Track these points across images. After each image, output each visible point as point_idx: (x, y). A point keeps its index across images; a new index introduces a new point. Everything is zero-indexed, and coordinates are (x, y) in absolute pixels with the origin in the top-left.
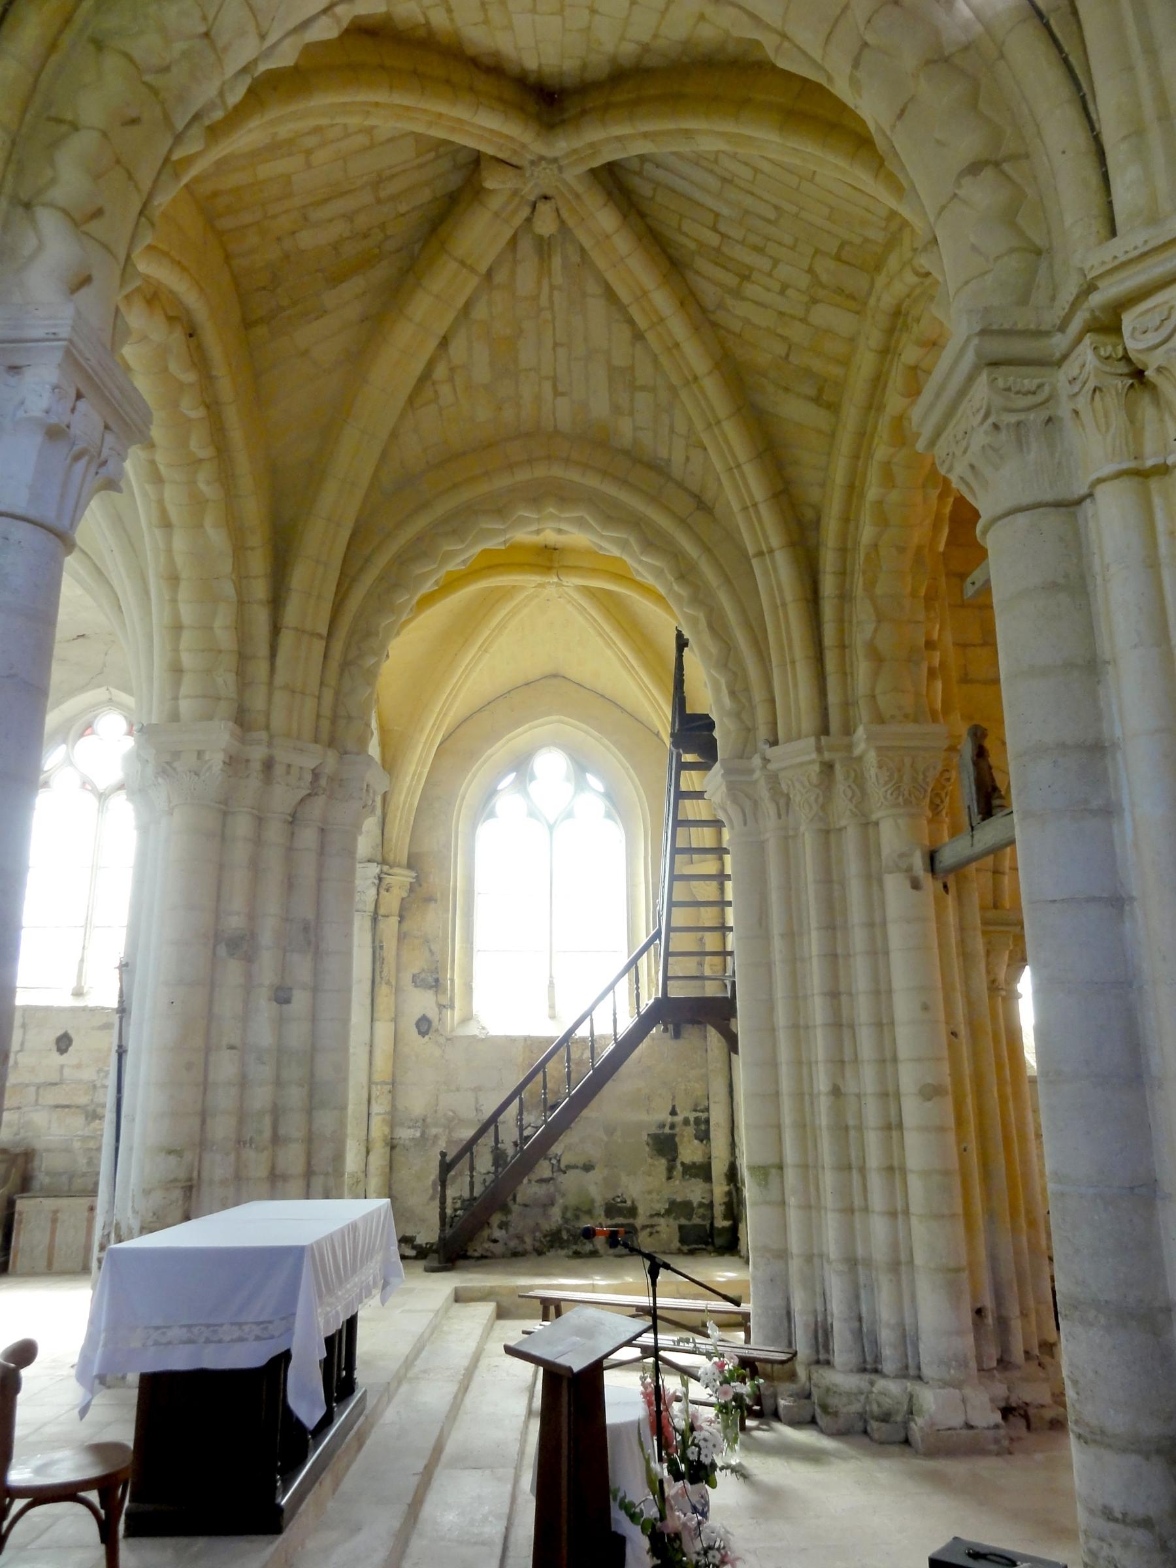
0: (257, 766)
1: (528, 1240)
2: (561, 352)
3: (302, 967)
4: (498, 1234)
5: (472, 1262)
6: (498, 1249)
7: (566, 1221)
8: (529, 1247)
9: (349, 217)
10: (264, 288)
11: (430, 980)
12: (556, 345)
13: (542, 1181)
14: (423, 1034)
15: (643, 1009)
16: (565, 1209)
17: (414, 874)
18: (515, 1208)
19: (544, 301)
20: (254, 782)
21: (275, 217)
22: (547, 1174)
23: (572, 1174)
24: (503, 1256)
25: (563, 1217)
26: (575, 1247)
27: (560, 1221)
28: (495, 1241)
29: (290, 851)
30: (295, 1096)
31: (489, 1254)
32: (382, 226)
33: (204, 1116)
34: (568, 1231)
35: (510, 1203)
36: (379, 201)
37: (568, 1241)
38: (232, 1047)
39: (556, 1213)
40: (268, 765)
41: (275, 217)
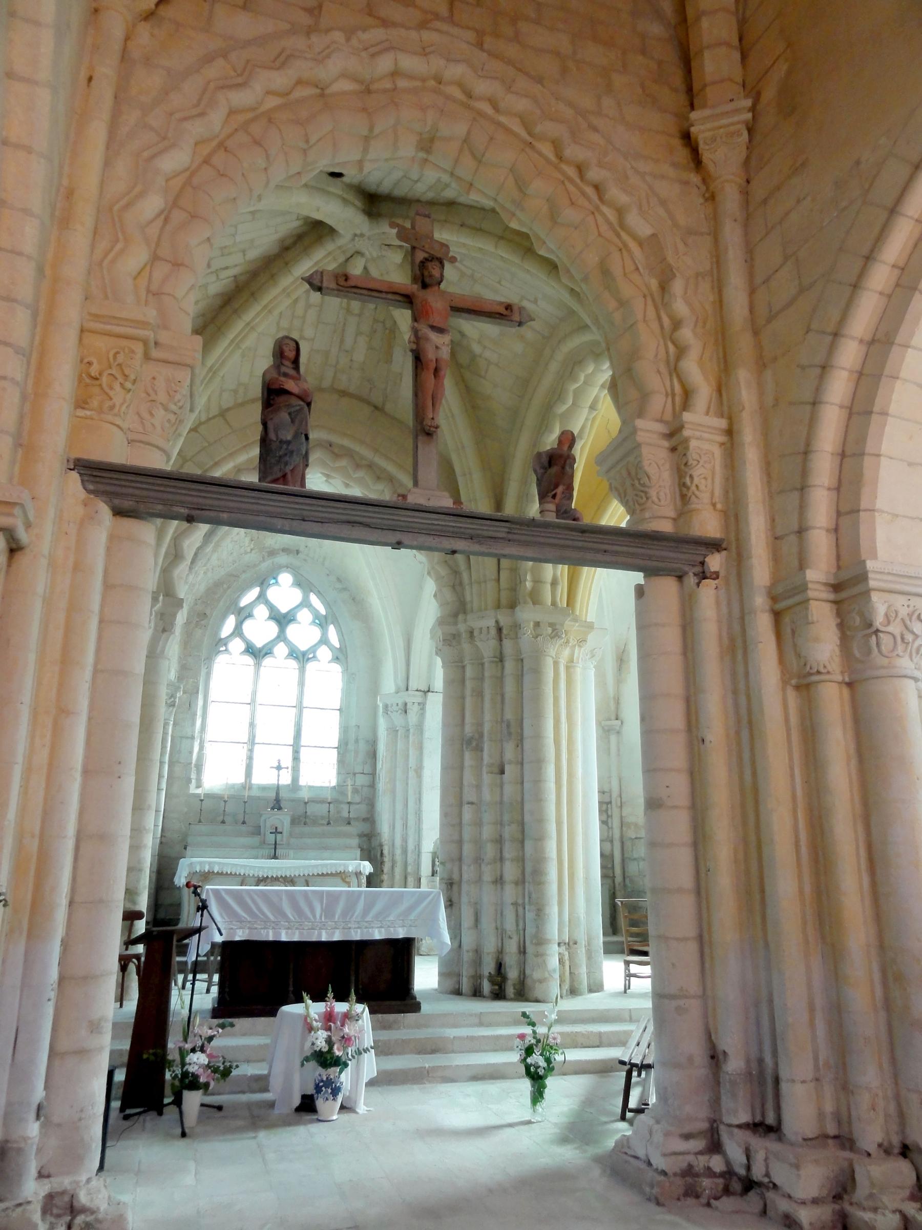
0: (464, 635)
2: (503, 283)
3: (510, 752)
9: (358, 333)
10: (371, 389)
12: (499, 282)
19: (469, 272)
20: (466, 646)
21: (338, 362)
29: (500, 680)
30: (509, 831)
32: (376, 321)
33: (460, 842)
36: (360, 315)
38: (472, 803)
40: (471, 633)
41: (338, 362)
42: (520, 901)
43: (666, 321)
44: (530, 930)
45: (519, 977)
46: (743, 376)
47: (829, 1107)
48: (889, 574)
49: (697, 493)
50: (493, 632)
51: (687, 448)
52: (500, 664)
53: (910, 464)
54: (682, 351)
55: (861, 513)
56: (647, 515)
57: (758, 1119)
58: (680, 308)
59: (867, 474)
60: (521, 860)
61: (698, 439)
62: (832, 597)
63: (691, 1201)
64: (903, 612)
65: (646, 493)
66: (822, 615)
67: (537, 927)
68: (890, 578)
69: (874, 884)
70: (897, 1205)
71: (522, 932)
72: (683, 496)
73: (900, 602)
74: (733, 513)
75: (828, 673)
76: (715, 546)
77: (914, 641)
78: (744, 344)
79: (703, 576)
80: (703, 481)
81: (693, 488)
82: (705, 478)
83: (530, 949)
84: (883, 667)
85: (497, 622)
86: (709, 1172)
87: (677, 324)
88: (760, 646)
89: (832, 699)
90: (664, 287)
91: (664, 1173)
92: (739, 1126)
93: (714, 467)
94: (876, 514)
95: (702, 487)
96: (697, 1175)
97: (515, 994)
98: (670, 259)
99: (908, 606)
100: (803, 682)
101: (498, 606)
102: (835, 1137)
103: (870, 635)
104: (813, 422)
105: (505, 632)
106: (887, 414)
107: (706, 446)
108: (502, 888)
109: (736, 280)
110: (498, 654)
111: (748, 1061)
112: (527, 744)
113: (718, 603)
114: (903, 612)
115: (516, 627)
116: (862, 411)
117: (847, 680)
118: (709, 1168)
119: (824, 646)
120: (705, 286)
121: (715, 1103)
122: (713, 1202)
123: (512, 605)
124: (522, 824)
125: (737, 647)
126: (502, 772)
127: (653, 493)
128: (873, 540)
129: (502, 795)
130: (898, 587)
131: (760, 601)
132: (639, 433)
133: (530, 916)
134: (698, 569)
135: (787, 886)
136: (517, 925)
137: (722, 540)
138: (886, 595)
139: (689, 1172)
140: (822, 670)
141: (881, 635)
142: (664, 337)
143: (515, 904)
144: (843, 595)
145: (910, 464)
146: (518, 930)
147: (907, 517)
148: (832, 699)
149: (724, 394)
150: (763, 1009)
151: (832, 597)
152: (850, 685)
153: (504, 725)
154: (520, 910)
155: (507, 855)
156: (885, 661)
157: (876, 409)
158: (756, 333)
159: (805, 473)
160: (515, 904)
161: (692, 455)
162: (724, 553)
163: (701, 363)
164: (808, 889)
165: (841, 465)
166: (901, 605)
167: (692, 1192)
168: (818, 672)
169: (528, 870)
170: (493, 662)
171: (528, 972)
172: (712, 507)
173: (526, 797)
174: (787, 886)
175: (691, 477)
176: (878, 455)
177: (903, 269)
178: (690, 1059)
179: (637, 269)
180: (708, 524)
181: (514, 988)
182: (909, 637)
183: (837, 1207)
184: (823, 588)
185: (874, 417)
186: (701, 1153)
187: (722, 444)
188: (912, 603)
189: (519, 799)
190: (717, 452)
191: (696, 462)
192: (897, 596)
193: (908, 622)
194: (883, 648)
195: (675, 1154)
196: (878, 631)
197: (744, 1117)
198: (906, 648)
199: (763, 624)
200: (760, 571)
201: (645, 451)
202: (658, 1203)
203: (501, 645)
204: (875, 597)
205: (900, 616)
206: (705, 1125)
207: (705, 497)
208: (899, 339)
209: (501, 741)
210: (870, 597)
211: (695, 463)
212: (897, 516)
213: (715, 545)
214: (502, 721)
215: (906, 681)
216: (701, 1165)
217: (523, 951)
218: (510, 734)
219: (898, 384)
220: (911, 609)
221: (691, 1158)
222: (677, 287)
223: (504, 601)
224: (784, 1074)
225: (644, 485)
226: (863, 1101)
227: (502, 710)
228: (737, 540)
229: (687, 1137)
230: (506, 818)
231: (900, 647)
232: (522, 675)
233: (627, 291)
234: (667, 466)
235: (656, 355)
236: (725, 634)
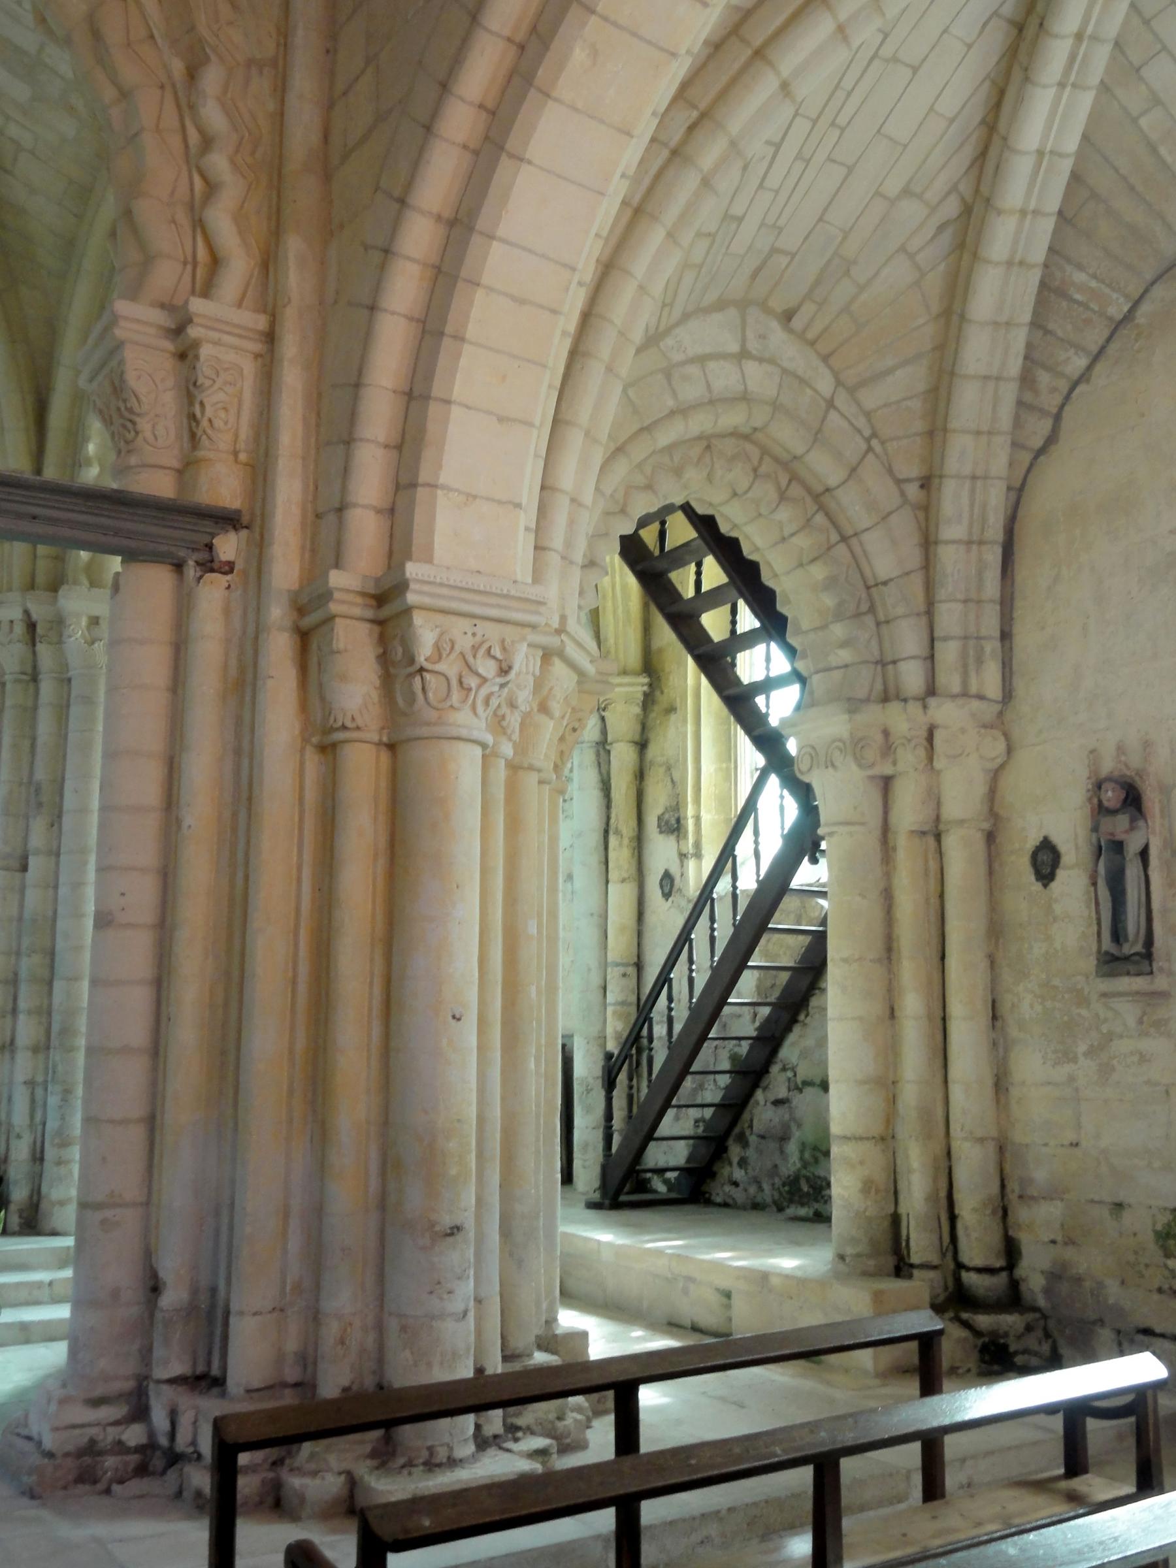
1: (766, 1187)
4: (738, 1174)
5: (715, 1210)
6: (738, 1195)
7: (805, 1165)
8: (769, 1200)
11: (673, 821)
13: (778, 1103)
14: (667, 895)
15: (786, 832)
16: (803, 1146)
17: (646, 680)
18: (752, 1139)
22: (782, 1093)
23: (809, 1092)
24: (744, 1208)
25: (801, 1159)
26: (816, 1206)
27: (799, 1165)
28: (736, 1184)
30: (29, 965)
31: (730, 1201)
34: (808, 1179)
35: (748, 1132)
37: (808, 1194)
39: (792, 1148)
42: (40, 1078)
43: (194, 136)
44: (52, 1125)
45: (31, 1197)
46: (294, 246)
47: (292, 1345)
48: (441, 585)
49: (209, 431)
50: (19, 629)
51: (197, 357)
52: (31, 685)
53: (501, 419)
54: (212, 188)
55: (419, 489)
56: (133, 460)
57: (201, 1369)
58: (214, 116)
59: (432, 427)
60: (45, 1012)
61: (217, 343)
62: (370, 614)
63: (82, 1488)
64: (464, 643)
65: (134, 423)
66: (353, 641)
67: (63, 1118)
68: (445, 591)
69: (387, 1036)
70: (345, 1466)
71: (40, 1128)
72: (193, 436)
73: (459, 629)
74: (259, 472)
75: (358, 728)
76: (229, 520)
77: (479, 687)
78: (304, 195)
79: (209, 565)
80: (223, 414)
81: (205, 423)
82: (225, 409)
83: (50, 1153)
84: (428, 724)
85: (27, 613)
86: (120, 1447)
87: (207, 142)
88: (270, 682)
89: (363, 766)
90: (192, 74)
91: (50, 1455)
92: (171, 1381)
93: (241, 392)
94: (439, 492)
95: (218, 423)
96: (101, 1453)
97: (21, 1225)
98: (203, 30)
99: (474, 634)
100: (326, 741)
101: (31, 586)
102: (296, 1385)
103: (411, 675)
104: (367, 337)
105: (40, 630)
106: (463, 339)
107: (229, 357)
108: (13, 1058)
109: (304, 82)
110: (29, 671)
111: (195, 1291)
112: (67, 820)
113: (227, 611)
114: (464, 643)
115: (59, 623)
116: (433, 330)
117: (385, 739)
118: (120, 1443)
119: (356, 690)
120: (262, 84)
121: (146, 1354)
122: (116, 1488)
123: (55, 586)
124: (52, 954)
125: (243, 684)
126: (24, 868)
127: (144, 425)
128: (430, 531)
129: (21, 906)
130: (454, 605)
131: (277, 612)
132: (122, 323)
133: (53, 1101)
134: (203, 556)
135: (269, 1041)
136: (32, 1117)
137: (238, 512)
138: (440, 618)
139: (91, 1449)
140: (349, 724)
141: (427, 676)
142: (188, 162)
143: (31, 1084)
144: (386, 611)
145: (501, 419)
146: (32, 1125)
147: (493, 500)
148: (363, 766)
149: (271, 269)
150: (219, 1218)
151: (370, 614)
152: (391, 747)
153: (32, 789)
154: (39, 1092)
155: (22, 1005)
156: (432, 715)
157: (449, 329)
158: (327, 177)
159: (352, 417)
160: (31, 1084)
161: (205, 369)
162: (244, 533)
163: (239, 218)
164: (301, 1043)
165: (407, 409)
166: (461, 633)
167: (87, 1477)
168: (344, 728)
169: (55, 1028)
170: (17, 681)
171: (44, 1190)
172: (231, 458)
173: (60, 910)
174: (269, 1041)
175: (202, 404)
176: (448, 402)
177: (493, 113)
178: (115, 1294)
179: (152, 37)
180: (223, 486)
181: (20, 1217)
182: (473, 682)
183: (271, 1475)
184: (359, 600)
185: (446, 342)
186: (116, 1423)
187: (257, 356)
188: (479, 630)
189: (50, 913)
190: (249, 368)
191: (211, 382)
192: (453, 619)
193: (471, 659)
194: (430, 695)
195: (74, 1427)
196: (422, 670)
197: (178, 1368)
198: (467, 696)
199: (279, 648)
200: (285, 569)
201: (129, 354)
202: (33, 1497)
203: (34, 653)
204: (418, 619)
205: (458, 648)
206: (130, 1385)
207: (223, 441)
208: (481, 224)
209: (27, 817)
210: (411, 618)
211: (208, 383)
212: (475, 497)
213: (232, 520)
214: (30, 782)
215: (461, 745)
216: (110, 1439)
217: (38, 1157)
218: (40, 805)
219: (480, 294)
220: (478, 638)
221: (93, 1431)
222: (212, 78)
223: (41, 579)
224: (234, 1307)
225: (130, 410)
226: (331, 1330)
227: (32, 763)
228: (263, 515)
229: (97, 1402)
230: (26, 942)
231: (456, 697)
232: (68, 706)
233: (129, 74)
234: (170, 383)
235: (173, 193)
236: (233, 662)
